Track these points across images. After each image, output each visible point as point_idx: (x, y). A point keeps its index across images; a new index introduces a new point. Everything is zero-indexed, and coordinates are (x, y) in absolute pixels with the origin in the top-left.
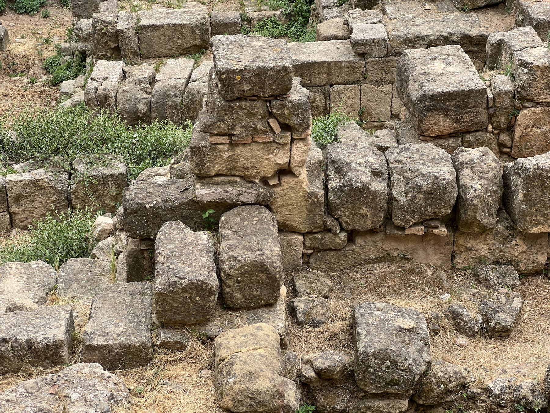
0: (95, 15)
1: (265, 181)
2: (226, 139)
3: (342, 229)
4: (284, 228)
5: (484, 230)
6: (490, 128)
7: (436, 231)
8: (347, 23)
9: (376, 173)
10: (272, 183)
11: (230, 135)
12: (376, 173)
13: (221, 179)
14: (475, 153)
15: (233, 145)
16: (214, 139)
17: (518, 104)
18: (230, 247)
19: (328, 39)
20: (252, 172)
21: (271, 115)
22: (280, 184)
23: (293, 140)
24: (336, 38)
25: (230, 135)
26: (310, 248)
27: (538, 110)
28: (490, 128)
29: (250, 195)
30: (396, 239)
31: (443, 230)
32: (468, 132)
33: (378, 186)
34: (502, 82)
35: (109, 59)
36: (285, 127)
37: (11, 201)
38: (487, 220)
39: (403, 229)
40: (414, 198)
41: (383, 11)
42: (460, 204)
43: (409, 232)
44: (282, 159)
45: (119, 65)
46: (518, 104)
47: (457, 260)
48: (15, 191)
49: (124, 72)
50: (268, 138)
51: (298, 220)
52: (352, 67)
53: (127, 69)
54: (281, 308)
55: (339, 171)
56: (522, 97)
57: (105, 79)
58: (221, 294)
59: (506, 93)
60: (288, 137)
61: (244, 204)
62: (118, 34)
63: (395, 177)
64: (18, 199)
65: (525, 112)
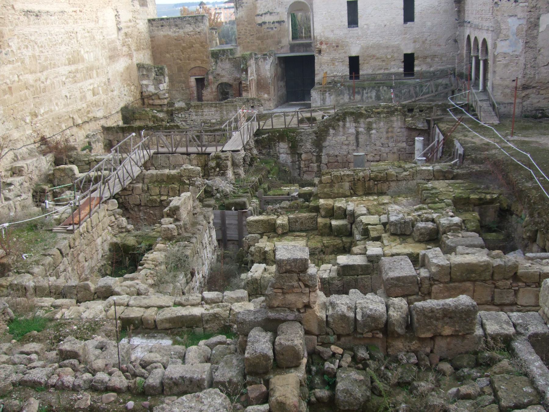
0: (256, 244)
1: (298, 310)
2: (280, 291)
3: (334, 334)
4: (307, 332)
5: (399, 336)
6: (420, 293)
7: (378, 336)
8: (365, 248)
9: (349, 308)
10: (302, 311)
11: (282, 289)
12: (349, 308)
13: (279, 309)
14: (396, 300)
15: (283, 293)
16: (275, 290)
17: (432, 282)
18: (280, 339)
19: (357, 254)
20: (292, 306)
21: (300, 280)
22: (305, 312)
23: (310, 292)
24: (360, 254)
25: (282, 289)
26: (320, 342)
27: (441, 285)
28: (420, 293)
29: (291, 316)
30: (360, 339)
31: (381, 335)
32: (410, 295)
33: (352, 315)
34: (424, 273)
35: (259, 263)
36: (306, 286)
37: (204, 323)
38: (400, 331)
39: (362, 334)
40: (366, 320)
41: (382, 242)
42: (387, 323)
43: (364, 336)
44: (306, 300)
45: (263, 266)
46: (432, 282)
47: (389, 350)
48: (206, 318)
49: (265, 269)
50: (299, 290)
51: (315, 328)
52: (366, 266)
53: (267, 267)
54: (303, 367)
55: (333, 308)
56: (432, 279)
57: (256, 271)
58: (275, 360)
59: (426, 277)
60: (307, 290)
61: (290, 321)
62: (266, 252)
63: (358, 310)
64: (207, 321)
65: (436, 286)
